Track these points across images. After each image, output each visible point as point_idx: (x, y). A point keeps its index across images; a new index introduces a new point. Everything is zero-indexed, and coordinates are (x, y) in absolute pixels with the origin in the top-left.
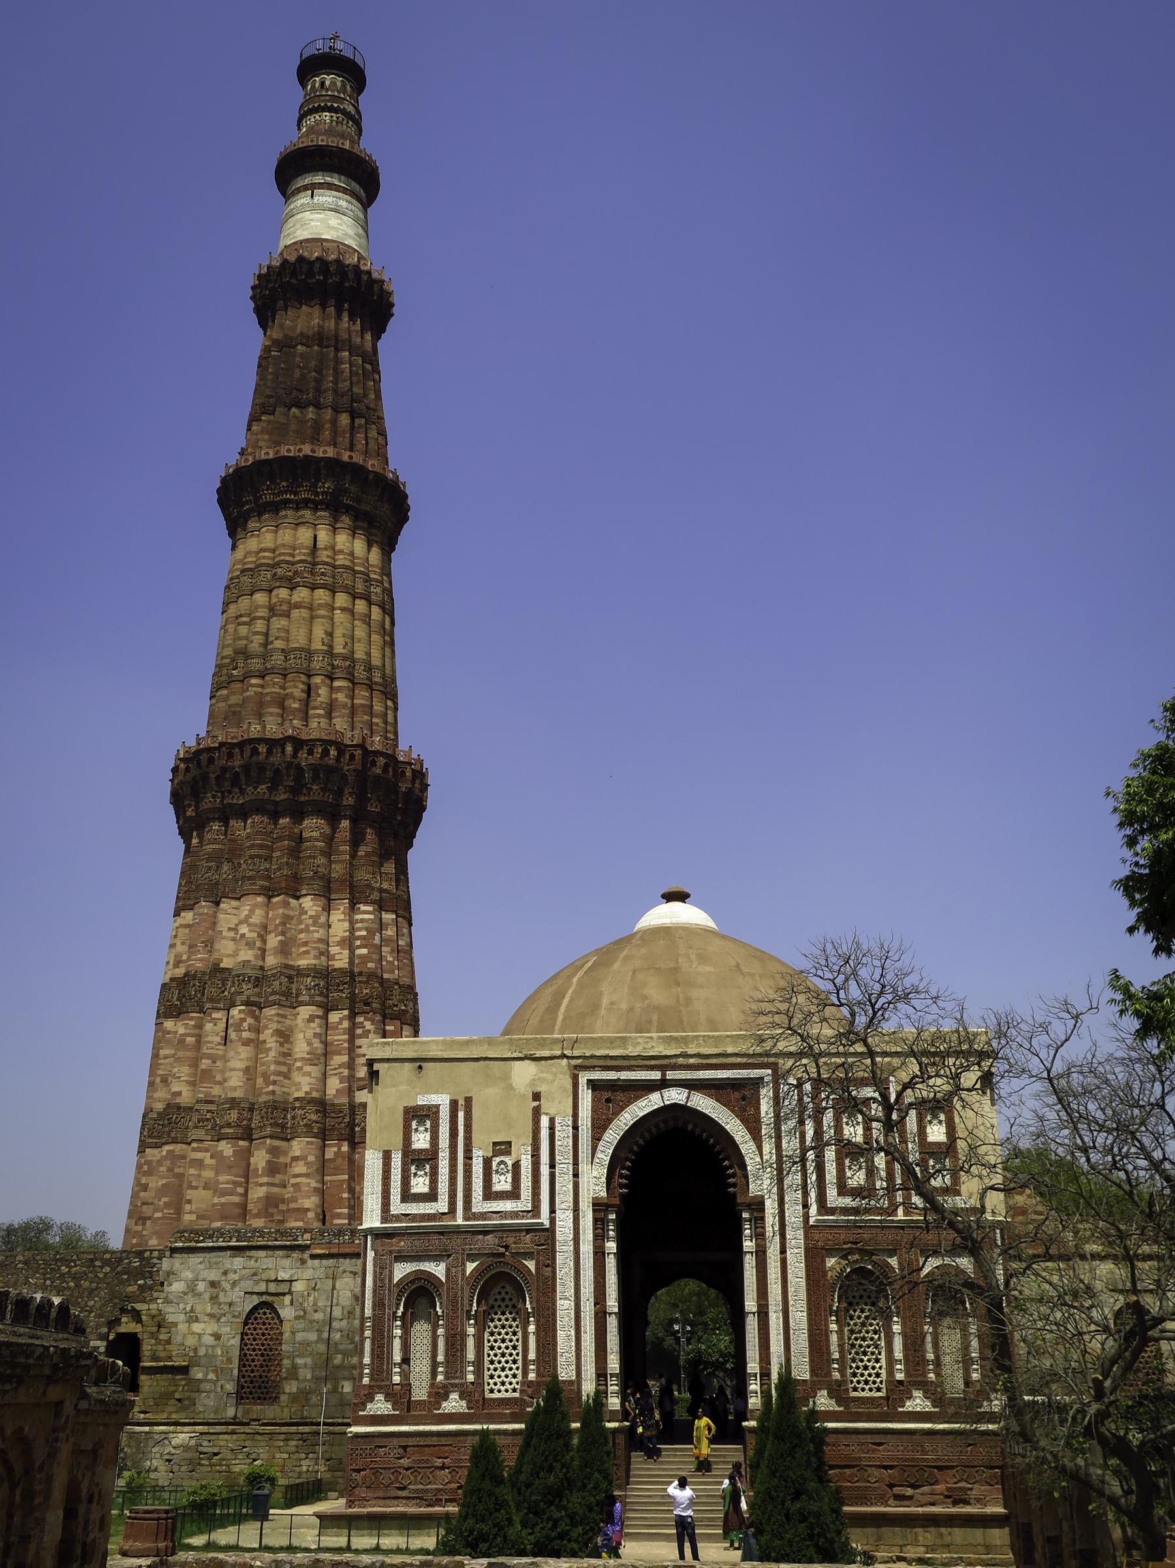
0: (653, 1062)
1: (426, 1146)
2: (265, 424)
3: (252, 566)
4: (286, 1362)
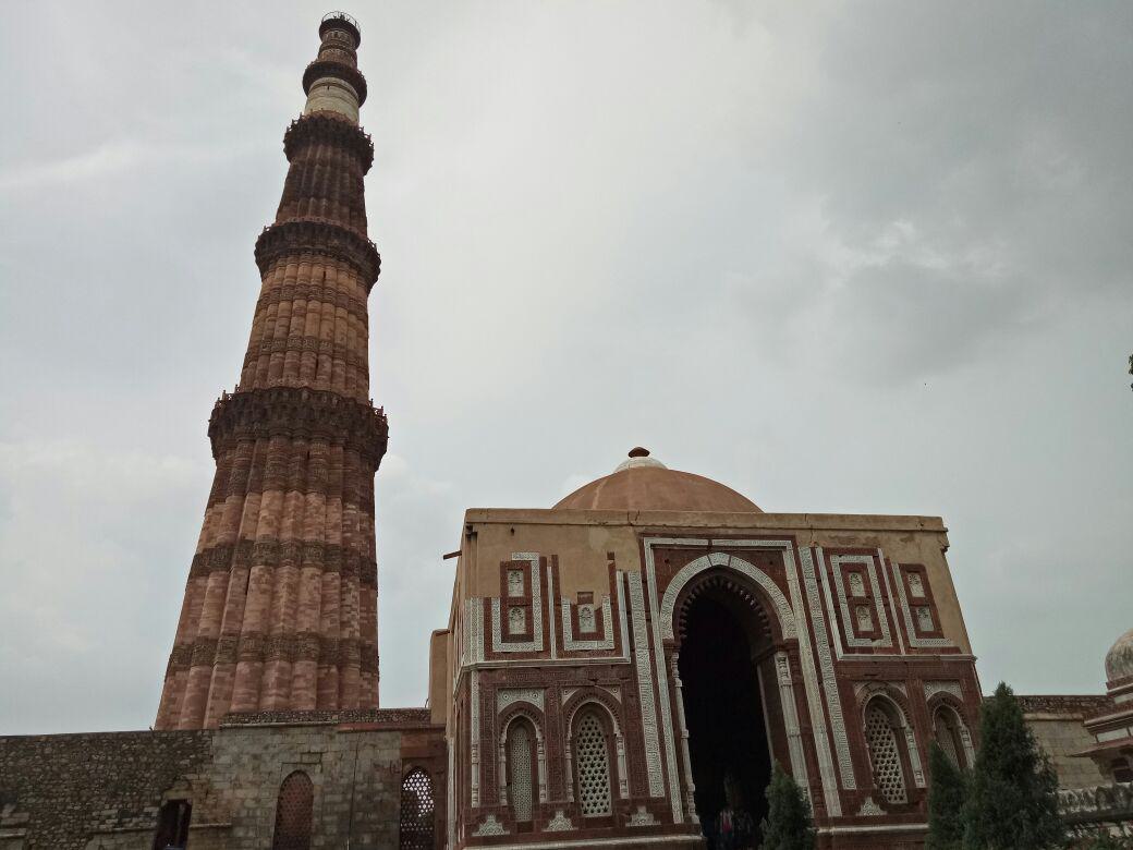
4: (316, 820)
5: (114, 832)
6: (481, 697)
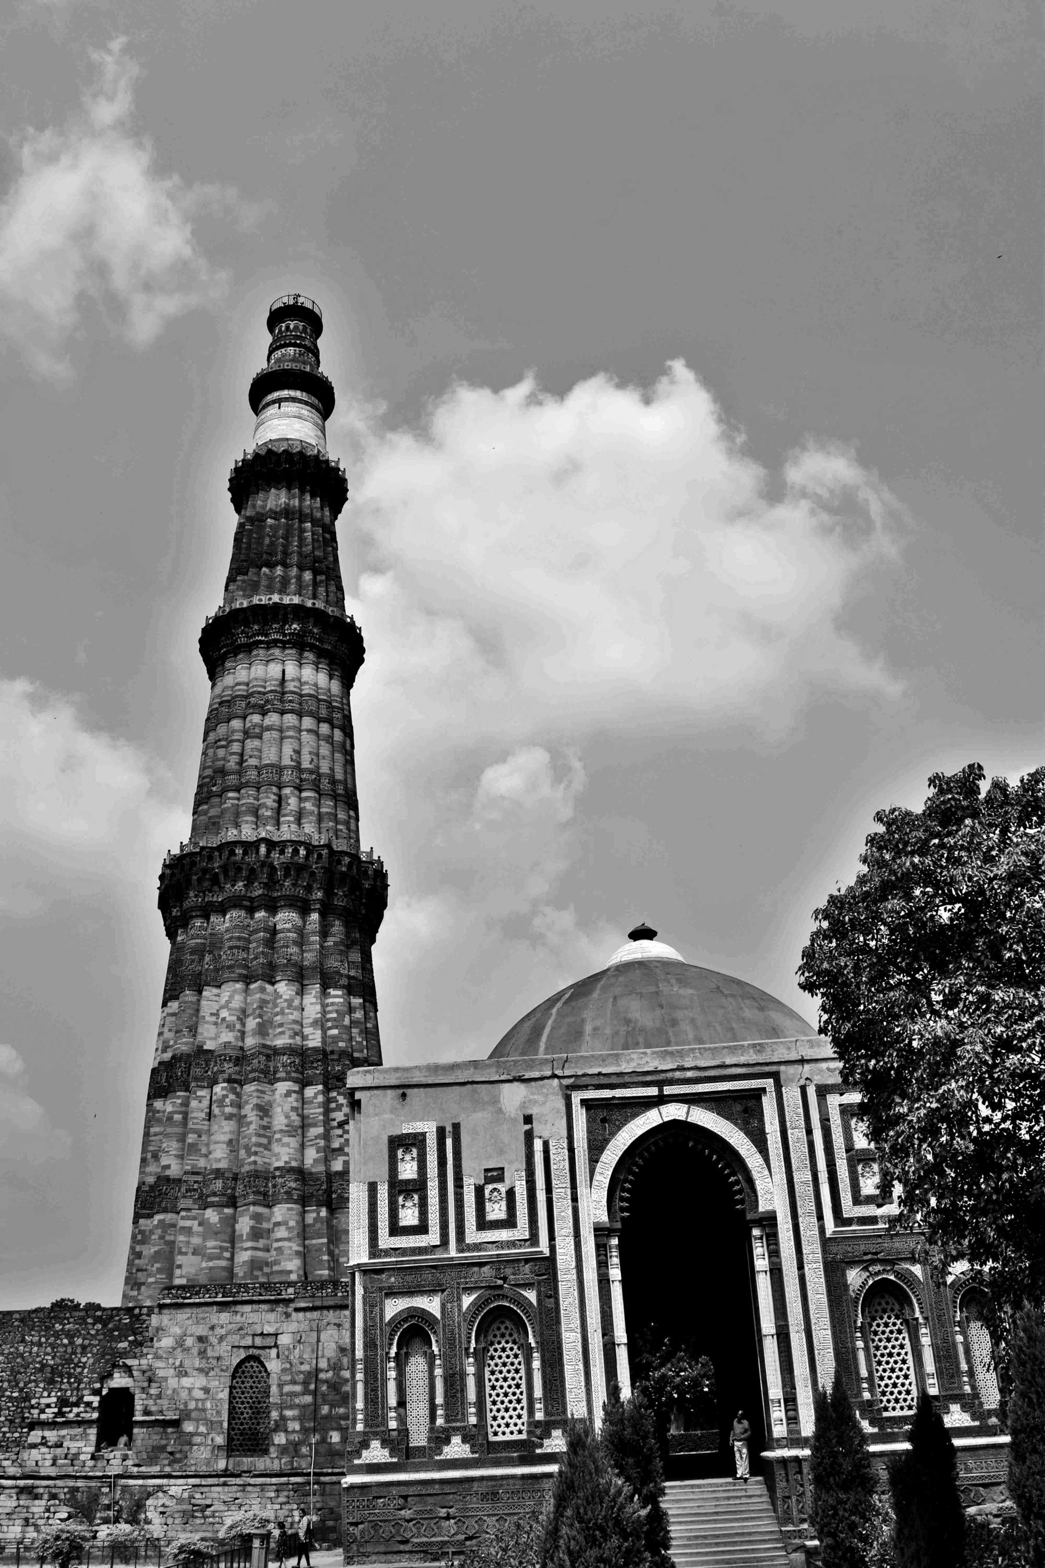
0: (649, 1078)
1: (415, 1176)
2: (240, 583)
3: (229, 698)
4: (274, 1414)
5: (52, 1425)
6: (364, 1304)
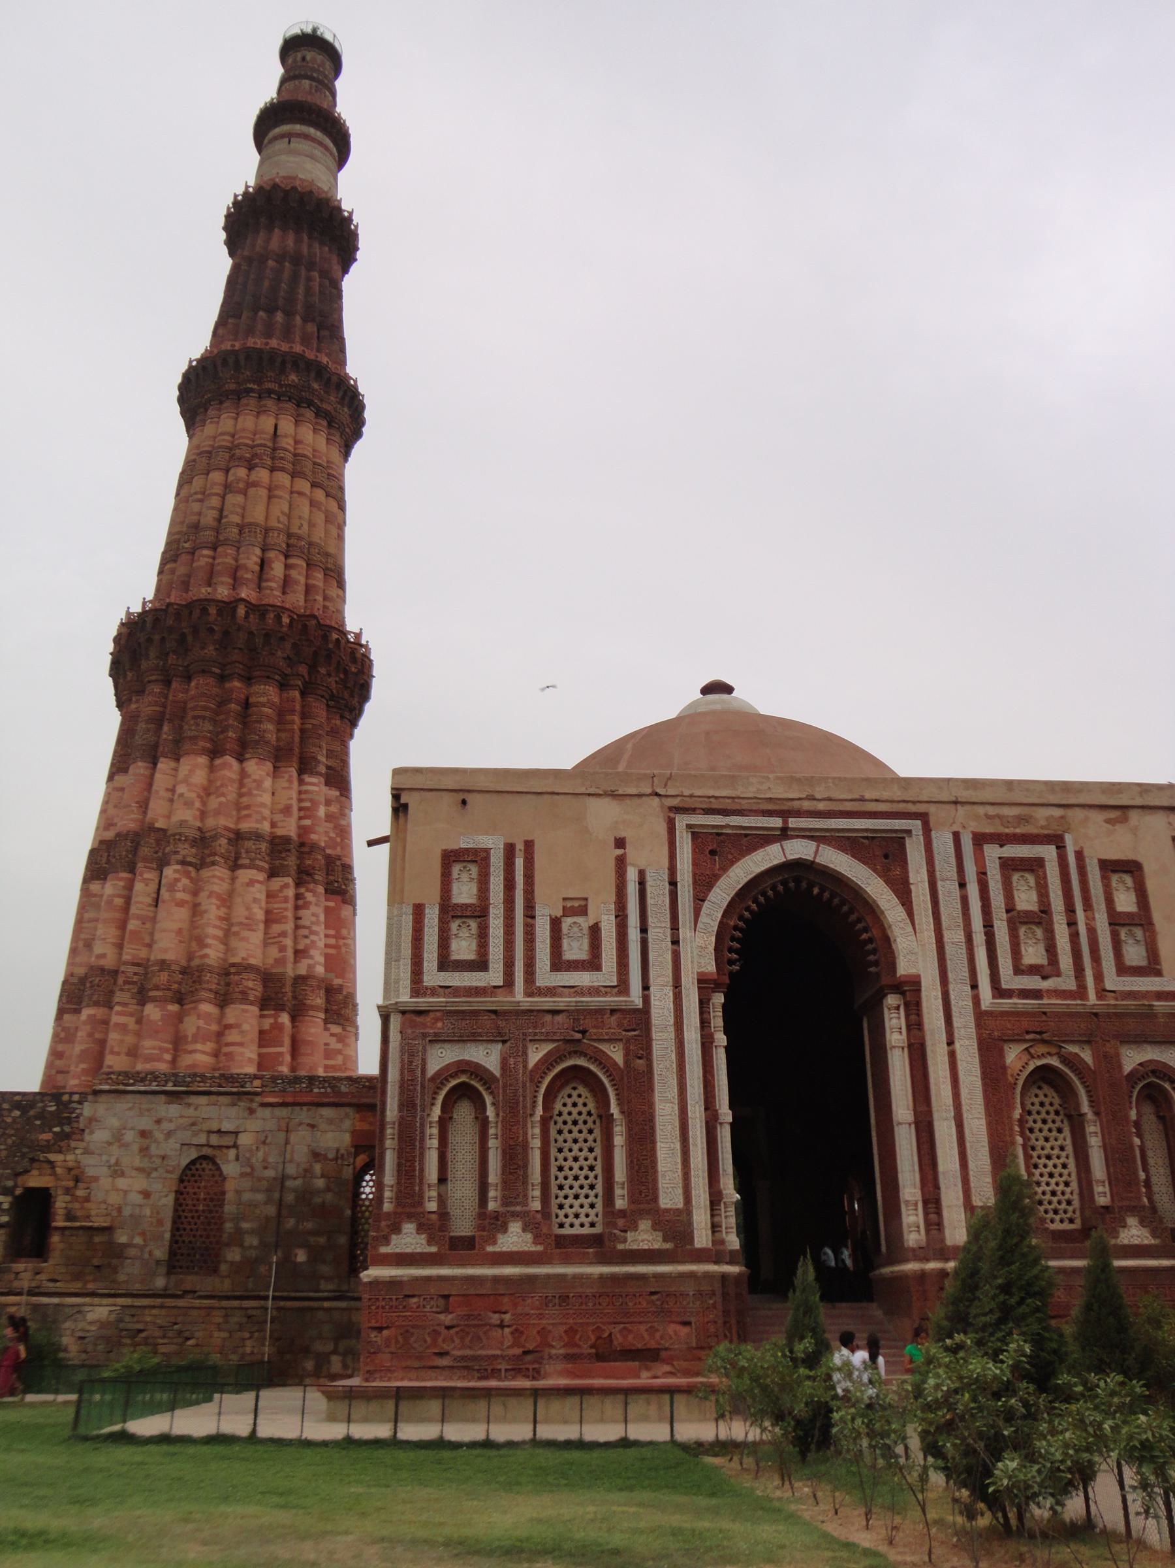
0: (770, 807)
4: (228, 1226)
6: (402, 1051)
